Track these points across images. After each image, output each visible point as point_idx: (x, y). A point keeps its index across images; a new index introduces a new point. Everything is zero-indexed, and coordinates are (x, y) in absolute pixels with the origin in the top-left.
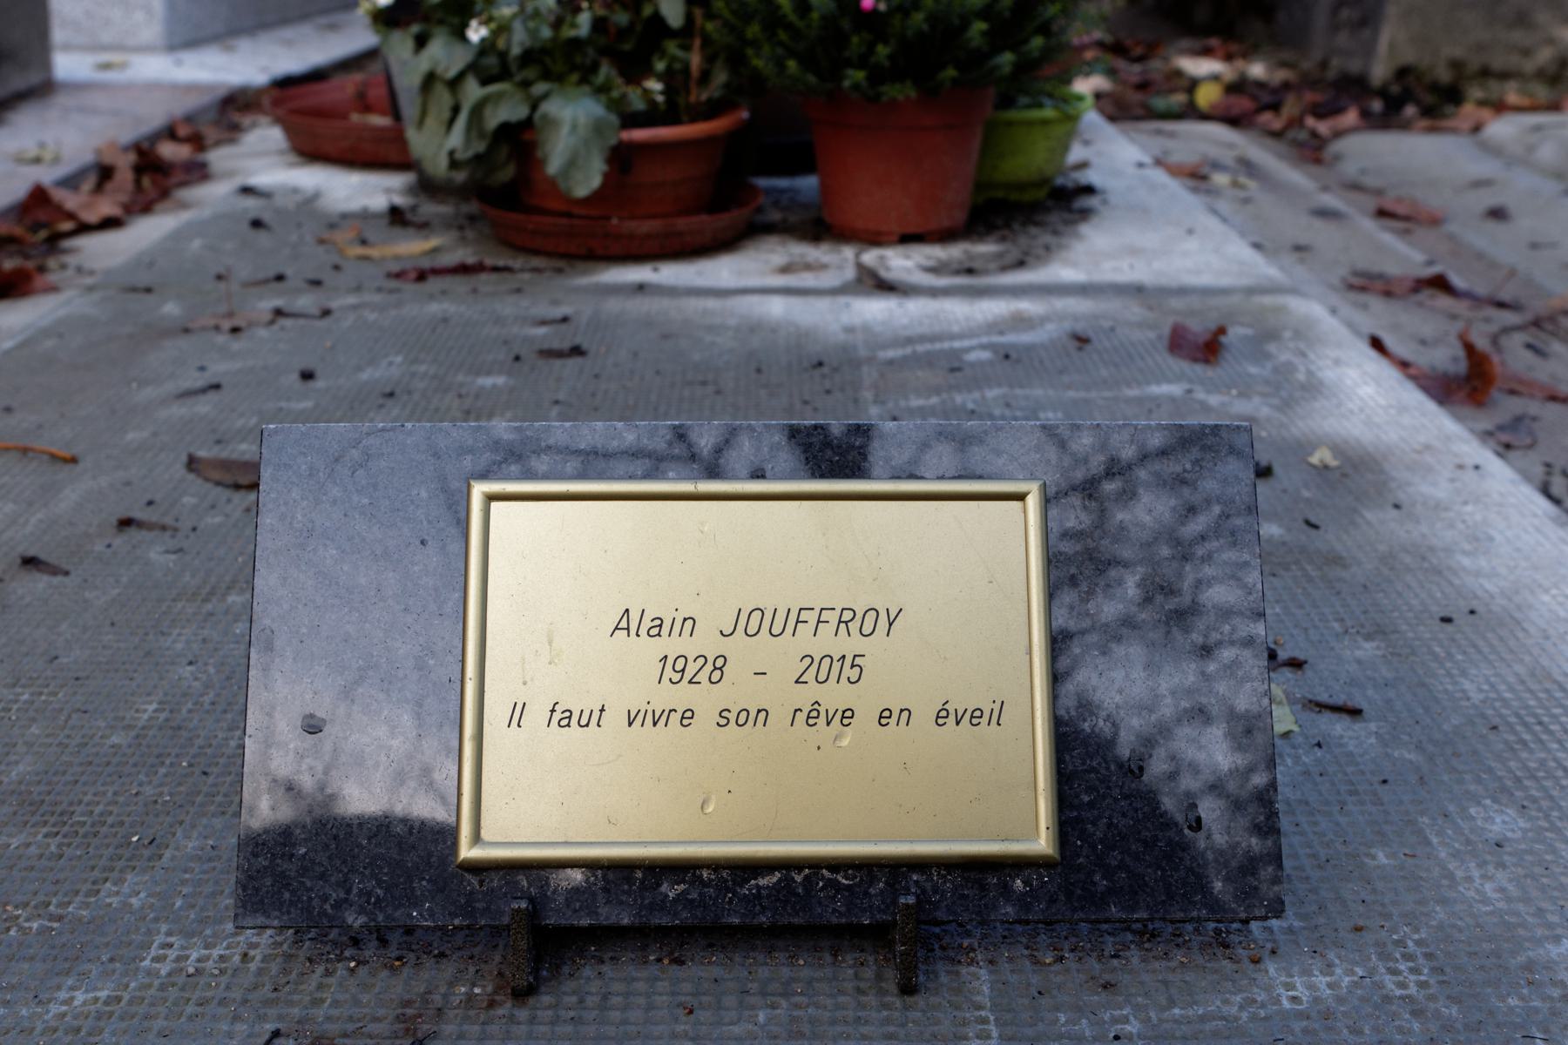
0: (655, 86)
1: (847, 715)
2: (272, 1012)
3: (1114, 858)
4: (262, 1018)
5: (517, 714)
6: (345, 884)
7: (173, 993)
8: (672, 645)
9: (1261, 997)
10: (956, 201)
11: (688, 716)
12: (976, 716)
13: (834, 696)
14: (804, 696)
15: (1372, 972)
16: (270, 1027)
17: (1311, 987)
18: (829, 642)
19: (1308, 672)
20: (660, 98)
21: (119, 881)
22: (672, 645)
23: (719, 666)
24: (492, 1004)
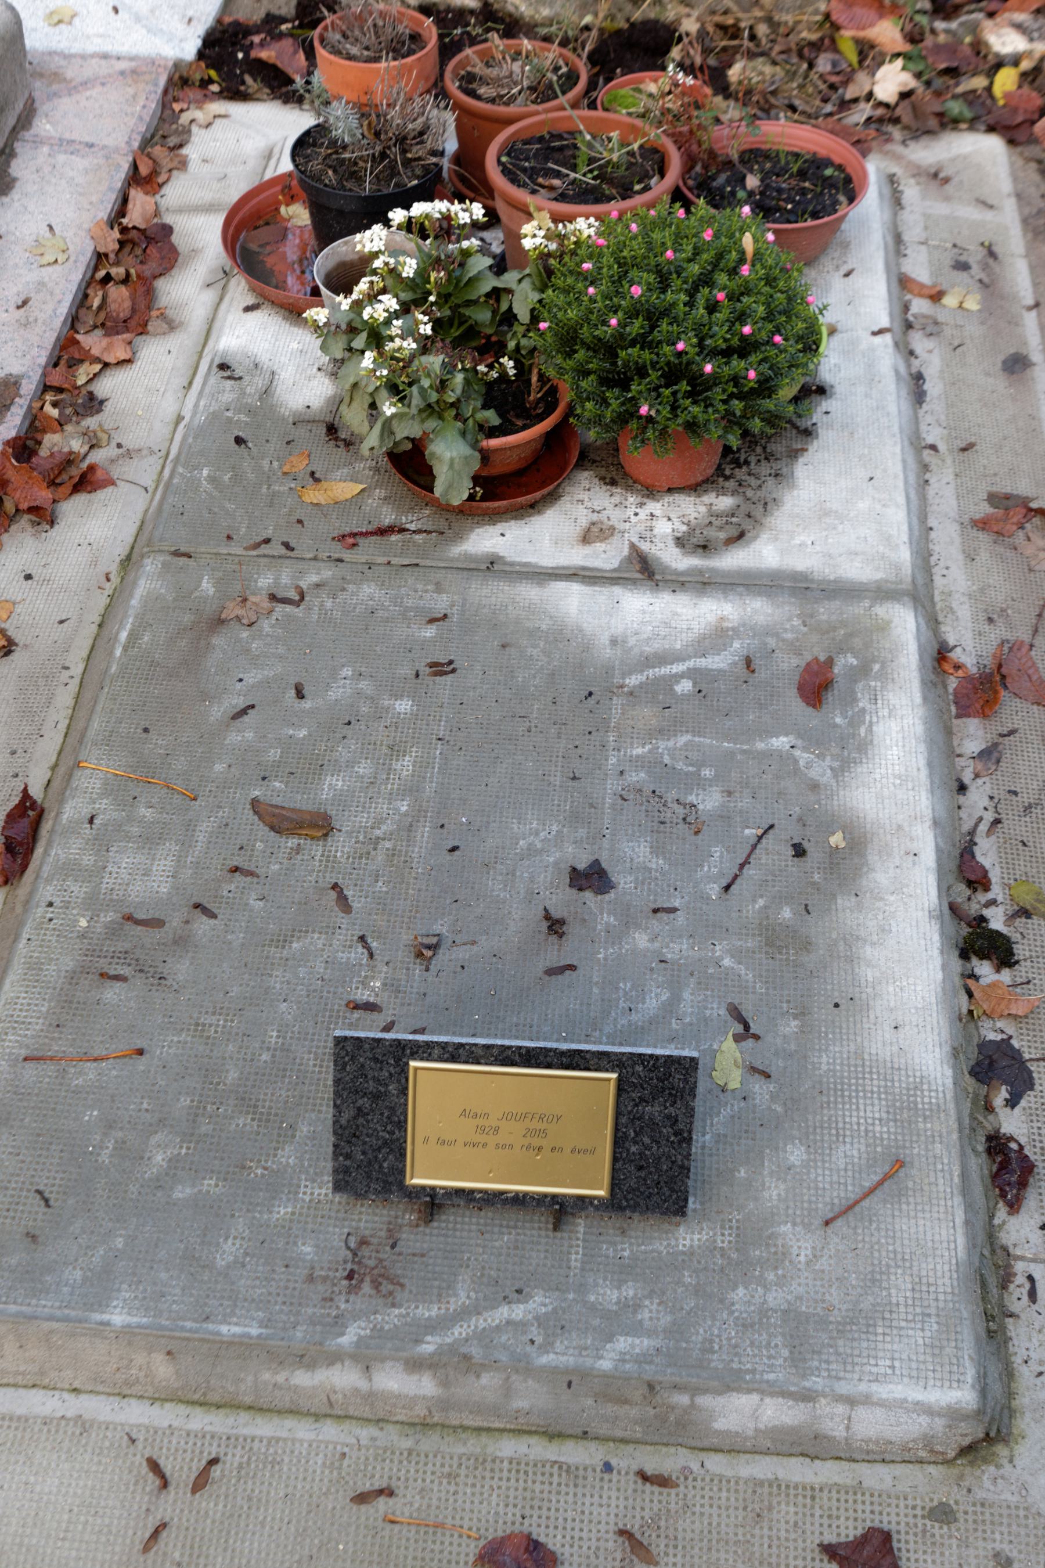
0: (509, 364)
1: (540, 1148)
2: (346, 1223)
3: (630, 1196)
4: (343, 1227)
5: (426, 1140)
6: (368, 1185)
7: (312, 1212)
8: (481, 1122)
9: (673, 1243)
10: (707, 466)
11: (485, 1145)
12: (585, 1151)
13: (536, 1142)
14: (526, 1142)
15: (715, 1235)
16: (346, 1230)
17: (692, 1240)
18: (536, 1125)
19: (760, 1042)
20: (512, 372)
21: (283, 1150)
22: (481, 1122)
23: (497, 1130)
24: (417, 1226)
